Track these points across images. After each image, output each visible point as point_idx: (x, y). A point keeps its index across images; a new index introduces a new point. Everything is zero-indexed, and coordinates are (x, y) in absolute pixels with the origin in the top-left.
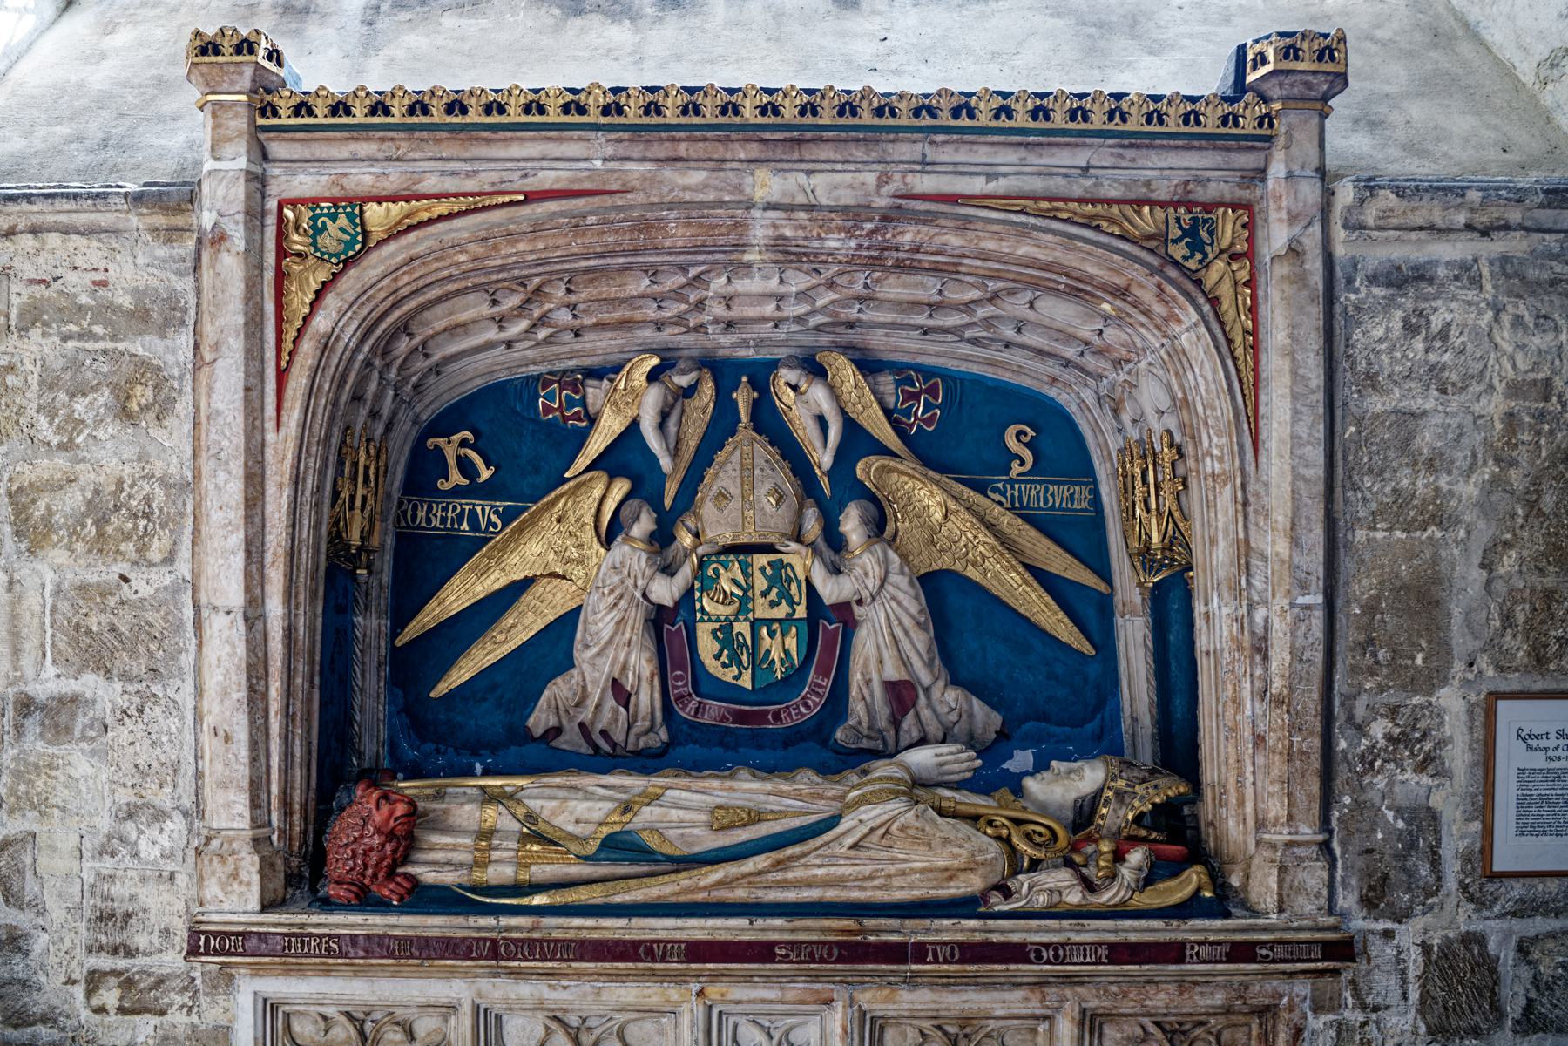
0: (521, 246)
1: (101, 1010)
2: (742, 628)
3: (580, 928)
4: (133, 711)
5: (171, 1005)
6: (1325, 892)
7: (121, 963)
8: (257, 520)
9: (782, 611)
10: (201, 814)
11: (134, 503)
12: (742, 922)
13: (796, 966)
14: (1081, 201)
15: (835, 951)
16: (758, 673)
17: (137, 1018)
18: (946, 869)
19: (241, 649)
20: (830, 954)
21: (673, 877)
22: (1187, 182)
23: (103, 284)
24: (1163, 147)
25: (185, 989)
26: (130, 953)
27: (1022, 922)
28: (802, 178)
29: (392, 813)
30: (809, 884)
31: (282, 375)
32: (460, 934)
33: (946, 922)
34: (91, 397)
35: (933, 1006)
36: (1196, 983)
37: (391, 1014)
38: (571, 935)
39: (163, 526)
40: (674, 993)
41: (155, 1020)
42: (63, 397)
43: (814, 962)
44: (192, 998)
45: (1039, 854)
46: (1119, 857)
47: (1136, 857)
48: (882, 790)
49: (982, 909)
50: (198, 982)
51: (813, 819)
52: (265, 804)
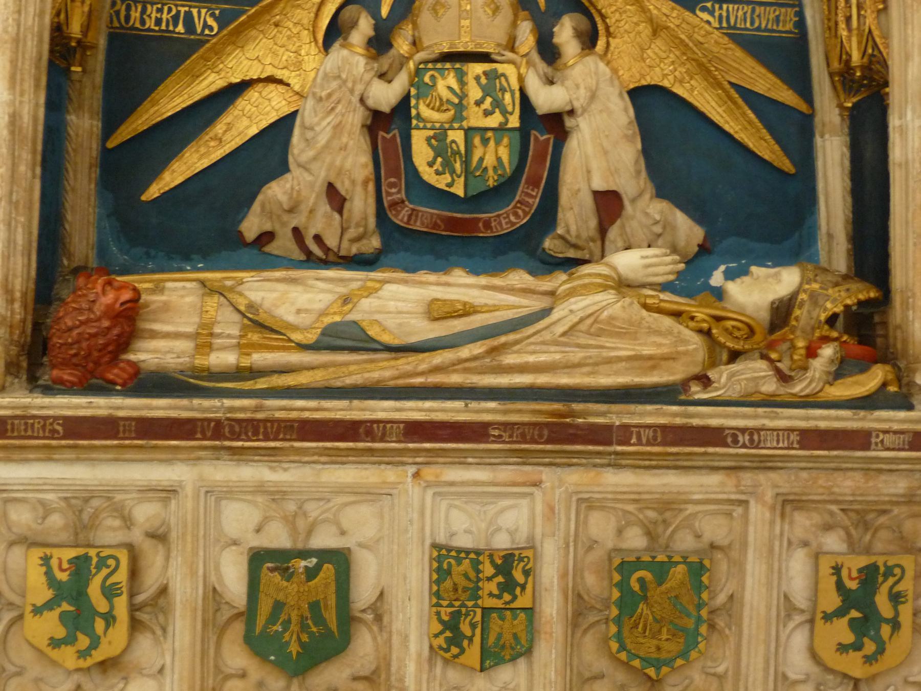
2: (456, 136)
9: (494, 121)
12: (459, 404)
13: (508, 446)
15: (546, 432)
16: (471, 178)
18: (650, 358)
20: (541, 436)
21: (393, 363)
27: (721, 409)
29: (116, 300)
30: (522, 369)
32: (185, 414)
33: (649, 408)
35: (635, 489)
36: (880, 471)
37: (109, 498)
38: (294, 415)
40: (390, 474)
43: (526, 442)
45: (738, 346)
46: (812, 353)
47: (828, 352)
48: (592, 284)
49: (683, 397)
51: (524, 312)
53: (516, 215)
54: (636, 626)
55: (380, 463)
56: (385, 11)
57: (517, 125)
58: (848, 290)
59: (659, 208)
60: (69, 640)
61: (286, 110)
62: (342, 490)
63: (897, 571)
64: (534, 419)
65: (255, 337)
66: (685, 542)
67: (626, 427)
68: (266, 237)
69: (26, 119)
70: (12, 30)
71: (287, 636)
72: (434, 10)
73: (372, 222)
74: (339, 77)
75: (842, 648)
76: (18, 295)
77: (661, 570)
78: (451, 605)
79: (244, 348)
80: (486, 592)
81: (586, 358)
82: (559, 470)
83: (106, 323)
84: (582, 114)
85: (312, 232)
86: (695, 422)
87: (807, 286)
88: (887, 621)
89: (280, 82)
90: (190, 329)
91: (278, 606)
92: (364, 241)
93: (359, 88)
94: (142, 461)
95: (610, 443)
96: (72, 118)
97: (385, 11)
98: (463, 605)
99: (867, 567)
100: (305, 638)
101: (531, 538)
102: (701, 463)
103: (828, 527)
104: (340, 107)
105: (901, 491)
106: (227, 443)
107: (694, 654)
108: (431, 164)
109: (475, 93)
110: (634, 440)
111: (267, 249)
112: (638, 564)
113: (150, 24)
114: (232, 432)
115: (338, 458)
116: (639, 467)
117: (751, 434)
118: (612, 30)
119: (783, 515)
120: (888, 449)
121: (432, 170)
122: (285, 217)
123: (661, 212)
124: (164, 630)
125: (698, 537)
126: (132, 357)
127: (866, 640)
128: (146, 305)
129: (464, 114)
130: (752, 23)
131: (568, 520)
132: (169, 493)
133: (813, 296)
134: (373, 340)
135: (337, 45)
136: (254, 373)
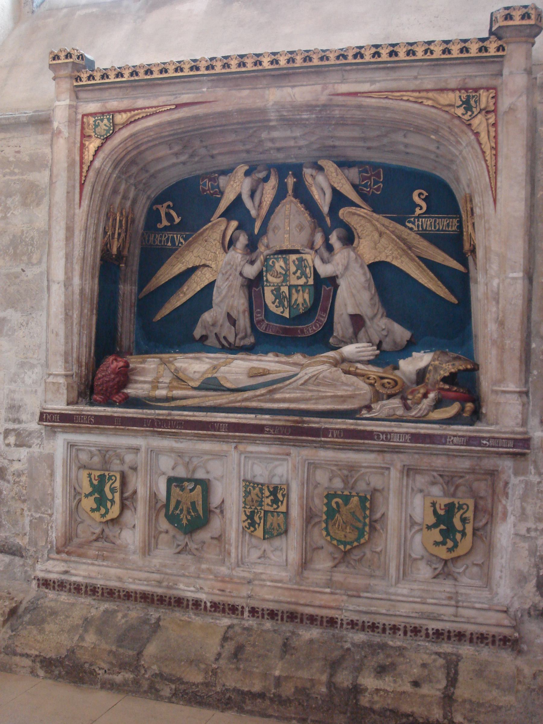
0: (175, 127)
1: (8, 445)
2: (285, 289)
3: (187, 416)
4: (24, 324)
5: (33, 443)
6: (520, 416)
7: (16, 426)
8: (71, 245)
9: (302, 281)
10: (47, 366)
11: (27, 240)
12: (253, 416)
14: (413, 91)
17: (21, 448)
18: (342, 396)
19: (63, 298)
22: (465, 79)
23: (18, 152)
24: (451, 64)
25: (39, 437)
26: (20, 422)
28: (289, 90)
29: (117, 366)
30: (284, 400)
31: (82, 185)
32: (140, 416)
33: (339, 420)
34: (14, 197)
39: (38, 249)
40: (225, 447)
41: (27, 450)
42: (3, 198)
44: (42, 441)
49: (358, 416)
50: (44, 434)
52: (70, 362)
53: (316, 326)
54: (335, 524)
55: (220, 441)
56: (256, 231)
57: (312, 283)
58: (453, 365)
59: (384, 322)
60: (98, 509)
61: (212, 279)
62: (206, 453)
63: (465, 507)
64: (289, 424)
65: (175, 384)
66: (362, 486)
67: (327, 429)
68: (204, 338)
69: (87, 290)
70: (82, 255)
71: (182, 516)
72: (274, 231)
73: (249, 330)
74: (230, 264)
75: (436, 544)
76: (84, 364)
77: (347, 499)
78: (250, 508)
79: (171, 388)
80: (266, 503)
81: (312, 396)
82: (298, 448)
83: (113, 376)
84: (341, 277)
85: (223, 335)
86: (361, 428)
87: (433, 363)
88: (459, 532)
89: (208, 266)
90: (149, 379)
91: (178, 503)
92: (247, 339)
93: (239, 269)
94: (124, 435)
95: (319, 436)
96: (121, 286)
97: (256, 231)
98: (256, 508)
99: (449, 504)
100: (189, 517)
101: (287, 481)
102: (363, 448)
103: (433, 483)
104: (231, 278)
105: (468, 467)
106: (156, 429)
107: (362, 541)
108: (273, 303)
109: (293, 268)
110: (330, 435)
111: (206, 343)
112: (335, 495)
113: (157, 243)
114: (158, 425)
115: (201, 438)
116: (335, 449)
117: (386, 435)
118: (360, 235)
119: (408, 475)
120: (455, 445)
121: (274, 306)
122: (211, 328)
123: (385, 324)
124: (135, 509)
125: (368, 484)
126: (125, 391)
127: (448, 540)
128: (133, 369)
129: (288, 278)
130: (435, 228)
131: (304, 472)
132: (136, 450)
133: (436, 368)
134: (222, 386)
135: (231, 249)
136: (174, 399)
